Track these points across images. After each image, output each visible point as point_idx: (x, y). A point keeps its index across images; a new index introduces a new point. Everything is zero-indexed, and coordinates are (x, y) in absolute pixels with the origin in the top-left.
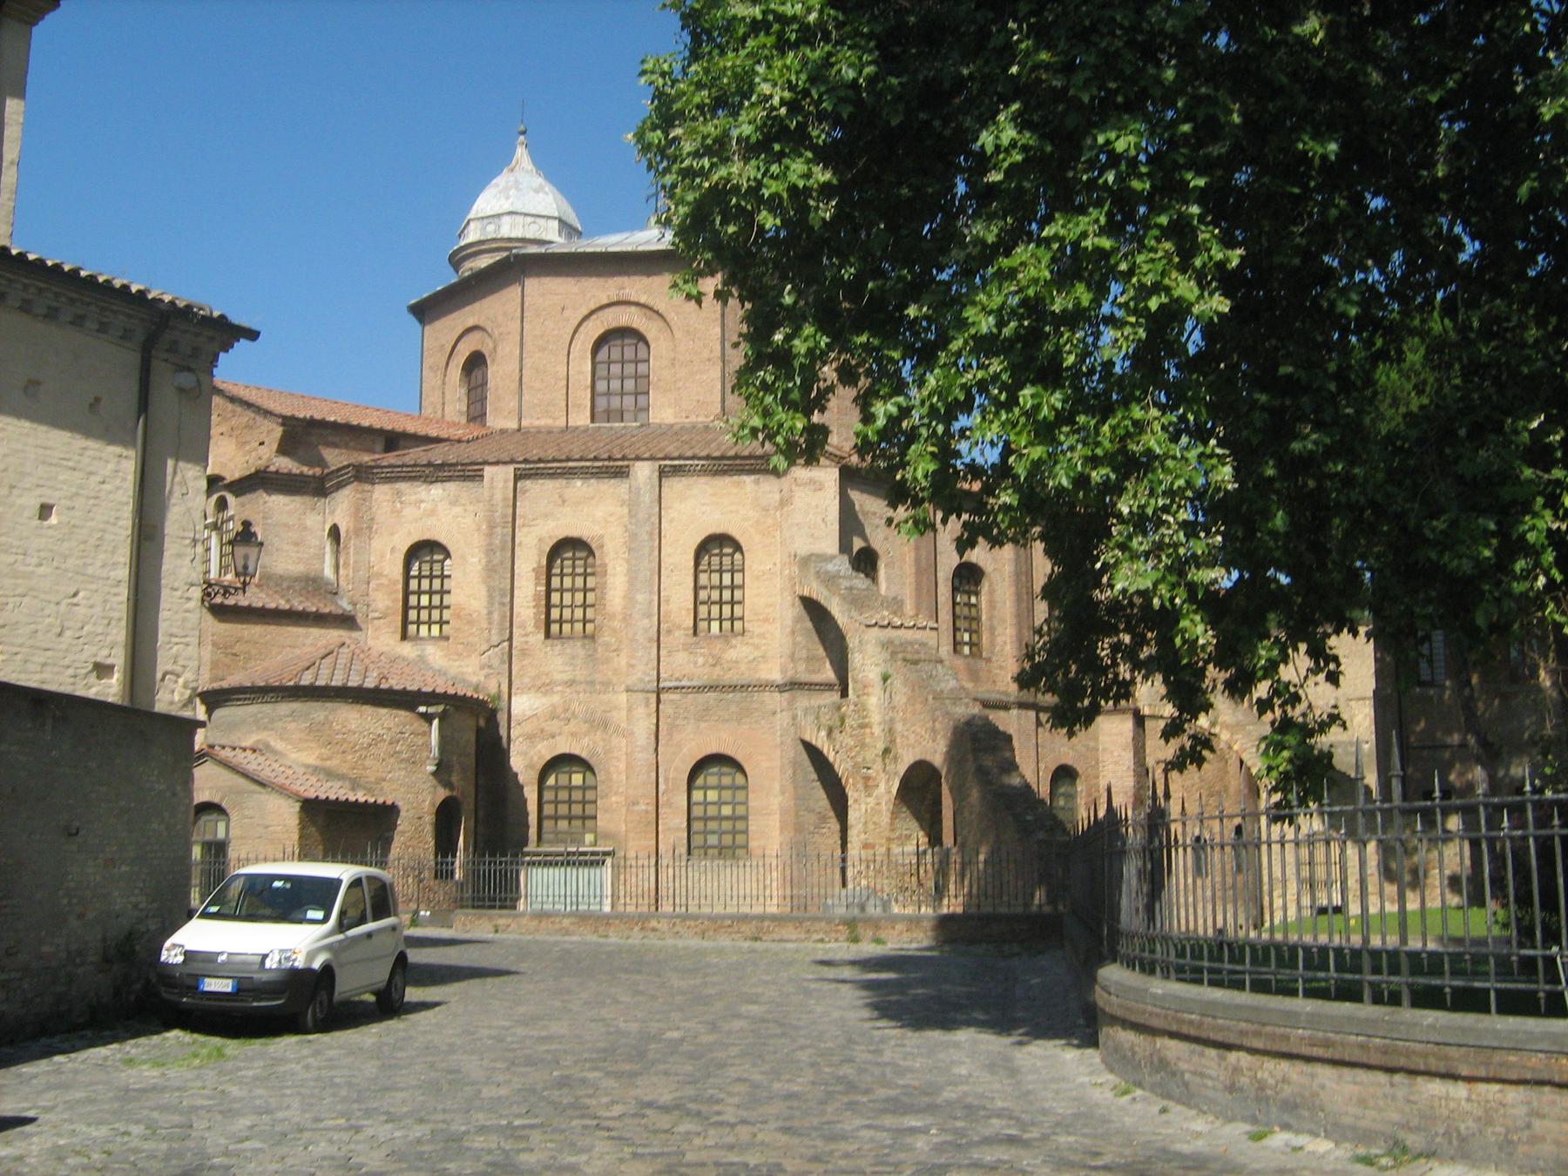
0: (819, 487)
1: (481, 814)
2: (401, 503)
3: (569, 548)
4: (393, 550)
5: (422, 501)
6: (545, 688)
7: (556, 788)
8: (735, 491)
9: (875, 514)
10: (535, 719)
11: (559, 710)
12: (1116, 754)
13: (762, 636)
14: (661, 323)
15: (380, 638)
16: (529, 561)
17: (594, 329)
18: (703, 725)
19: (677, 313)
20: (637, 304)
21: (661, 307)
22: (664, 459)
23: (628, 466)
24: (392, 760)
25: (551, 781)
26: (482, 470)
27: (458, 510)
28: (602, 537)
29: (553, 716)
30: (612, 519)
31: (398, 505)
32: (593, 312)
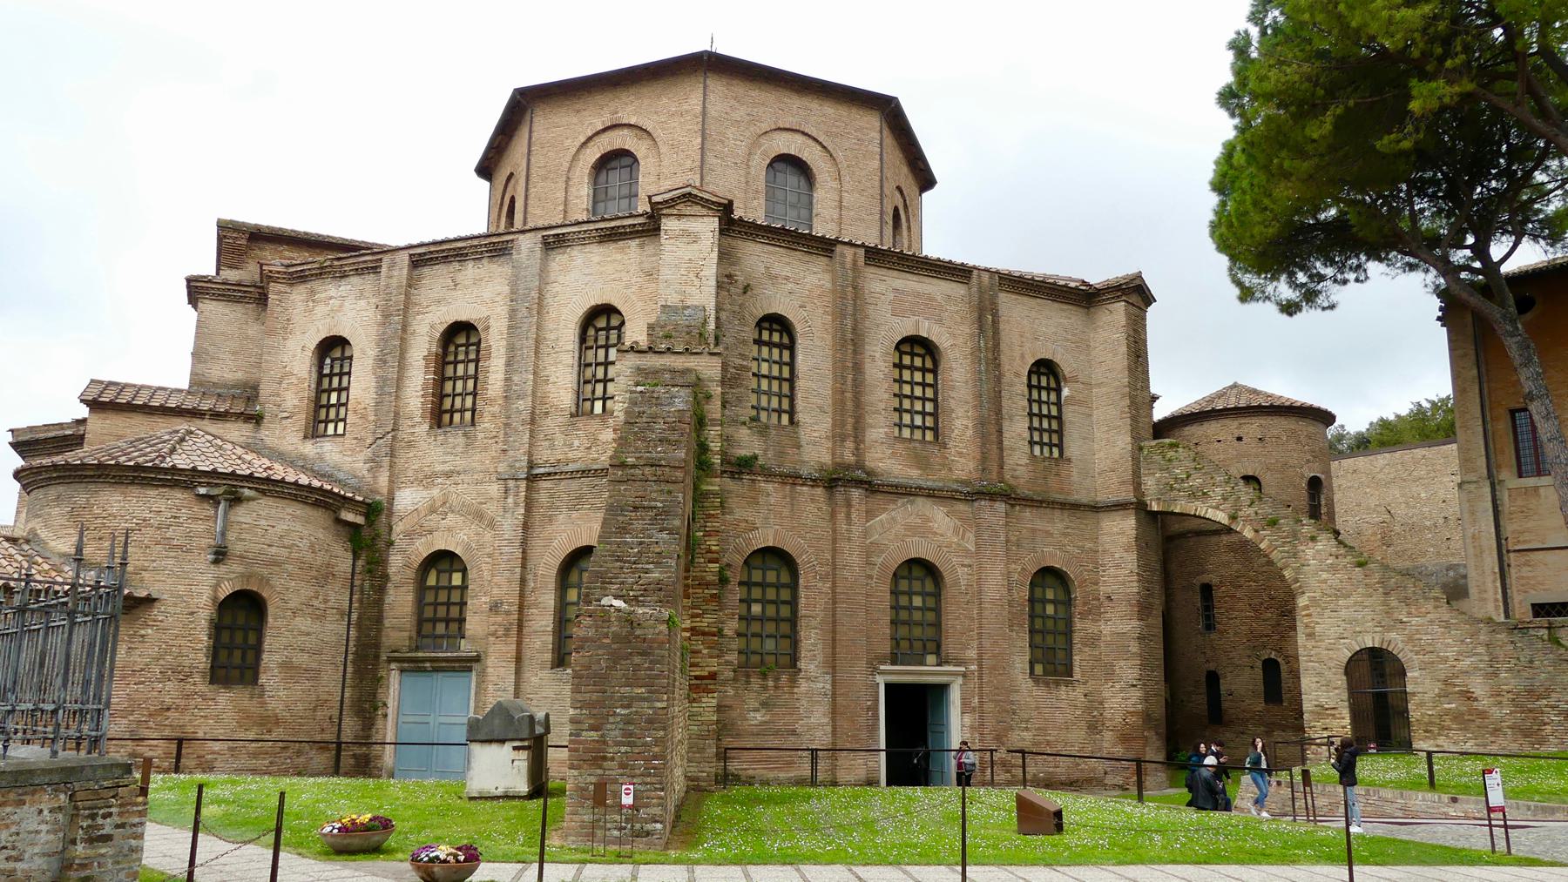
0: (693, 238)
1: (354, 616)
2: (313, 301)
3: (460, 333)
5: (331, 298)
6: (426, 480)
7: (437, 588)
8: (619, 257)
9: (787, 278)
10: (415, 514)
11: (439, 503)
12: (1117, 556)
15: (286, 435)
16: (422, 345)
17: (593, 154)
18: (575, 515)
20: (630, 126)
21: (649, 126)
22: (546, 229)
23: (512, 241)
24: (159, 548)
25: (432, 580)
26: (381, 259)
27: (362, 303)
28: (488, 318)
29: (433, 510)
32: (590, 139)
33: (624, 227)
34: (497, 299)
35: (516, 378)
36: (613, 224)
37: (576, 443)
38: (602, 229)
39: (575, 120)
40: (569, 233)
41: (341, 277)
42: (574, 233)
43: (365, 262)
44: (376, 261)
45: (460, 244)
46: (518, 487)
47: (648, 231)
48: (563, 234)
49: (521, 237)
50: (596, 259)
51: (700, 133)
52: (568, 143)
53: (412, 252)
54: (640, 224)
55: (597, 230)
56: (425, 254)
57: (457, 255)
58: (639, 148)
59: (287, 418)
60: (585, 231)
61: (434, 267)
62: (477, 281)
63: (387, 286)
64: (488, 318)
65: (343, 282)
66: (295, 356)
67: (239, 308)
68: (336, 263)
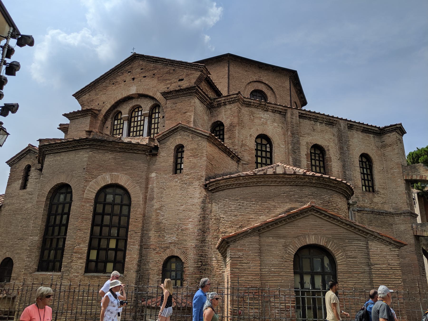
4: (251, 135)
5: (261, 118)
13: (383, 194)
14: (271, 92)
19: (277, 90)
20: (265, 84)
26: (287, 110)
28: (328, 146)
30: (331, 140)
31: (252, 117)
32: (250, 82)
33: (371, 129)
34: (331, 140)
35: (347, 172)
36: (369, 127)
37: (366, 201)
38: (365, 128)
39: (245, 73)
40: (355, 125)
41: (265, 111)
42: (357, 126)
43: (279, 108)
44: (285, 110)
45: (318, 115)
46: (355, 214)
47: (377, 133)
48: (353, 125)
49: (340, 121)
50: (361, 137)
51: (289, 96)
52: (243, 81)
53: (299, 111)
54: (376, 130)
55: (363, 127)
56: (304, 114)
57: (314, 119)
58: (268, 93)
59: (246, 164)
60: (360, 126)
61: (305, 120)
62: (322, 131)
63: (291, 122)
64: (328, 146)
65: (266, 113)
66: (247, 137)
67: (203, 105)
68: (267, 104)
